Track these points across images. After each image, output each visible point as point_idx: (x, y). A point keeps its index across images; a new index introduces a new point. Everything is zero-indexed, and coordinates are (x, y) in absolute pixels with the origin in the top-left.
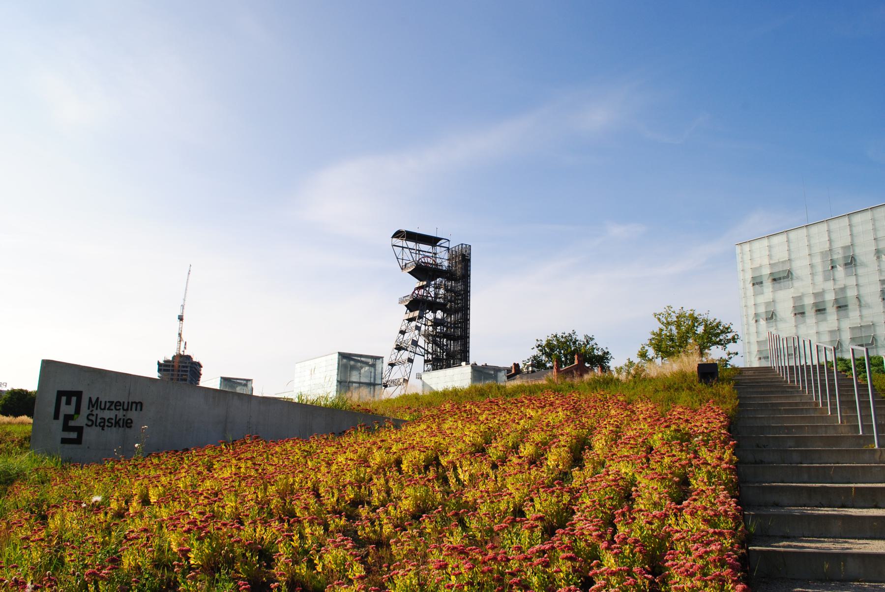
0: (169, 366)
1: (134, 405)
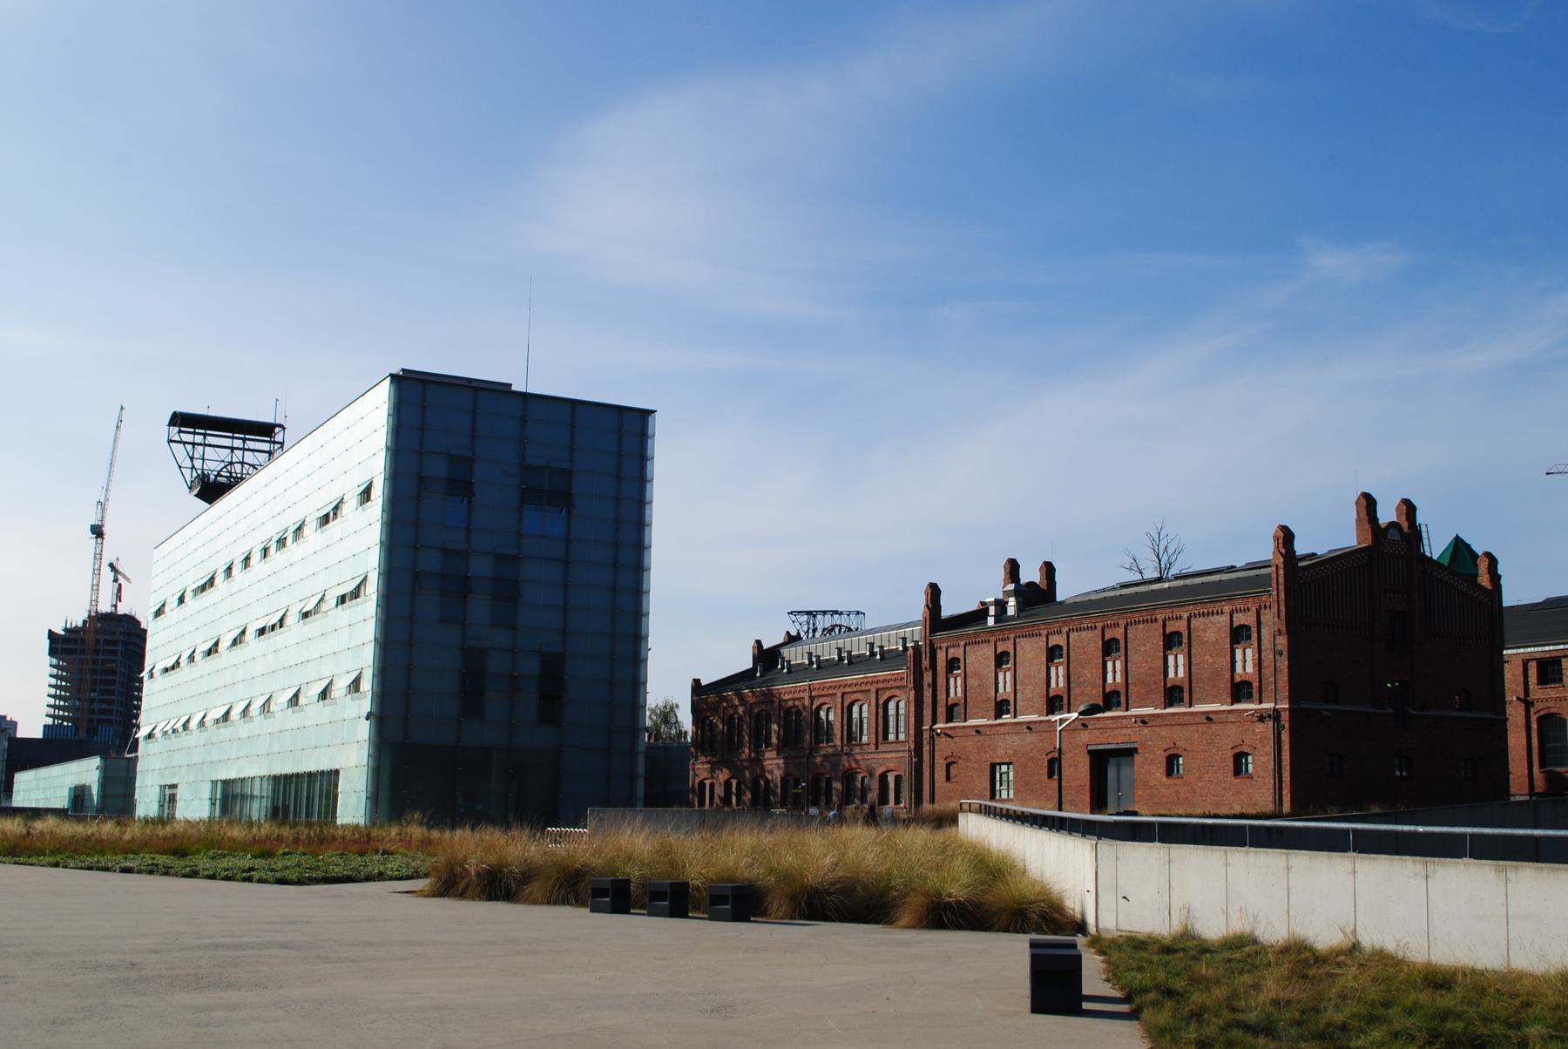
0: (75, 641)
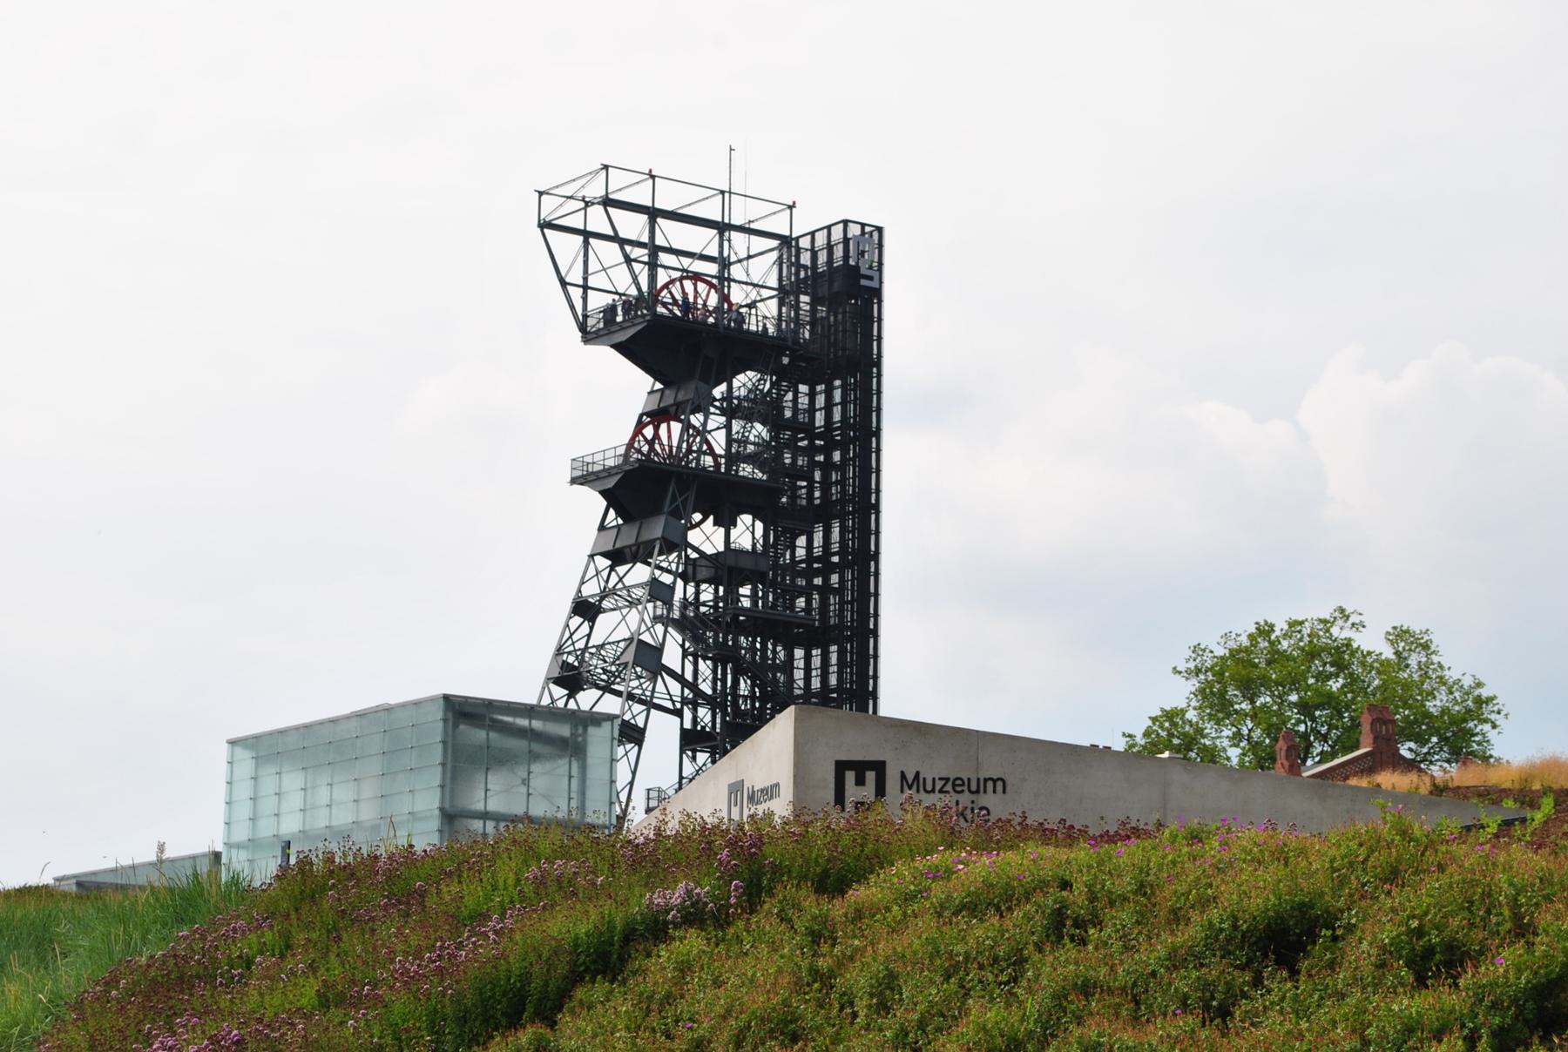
1: (990, 784)
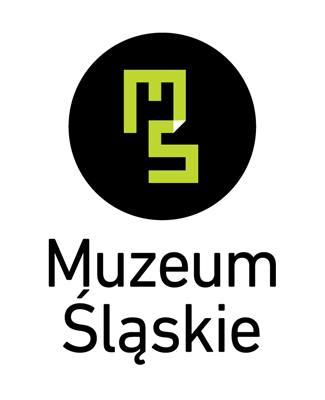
1: (242, 265)
